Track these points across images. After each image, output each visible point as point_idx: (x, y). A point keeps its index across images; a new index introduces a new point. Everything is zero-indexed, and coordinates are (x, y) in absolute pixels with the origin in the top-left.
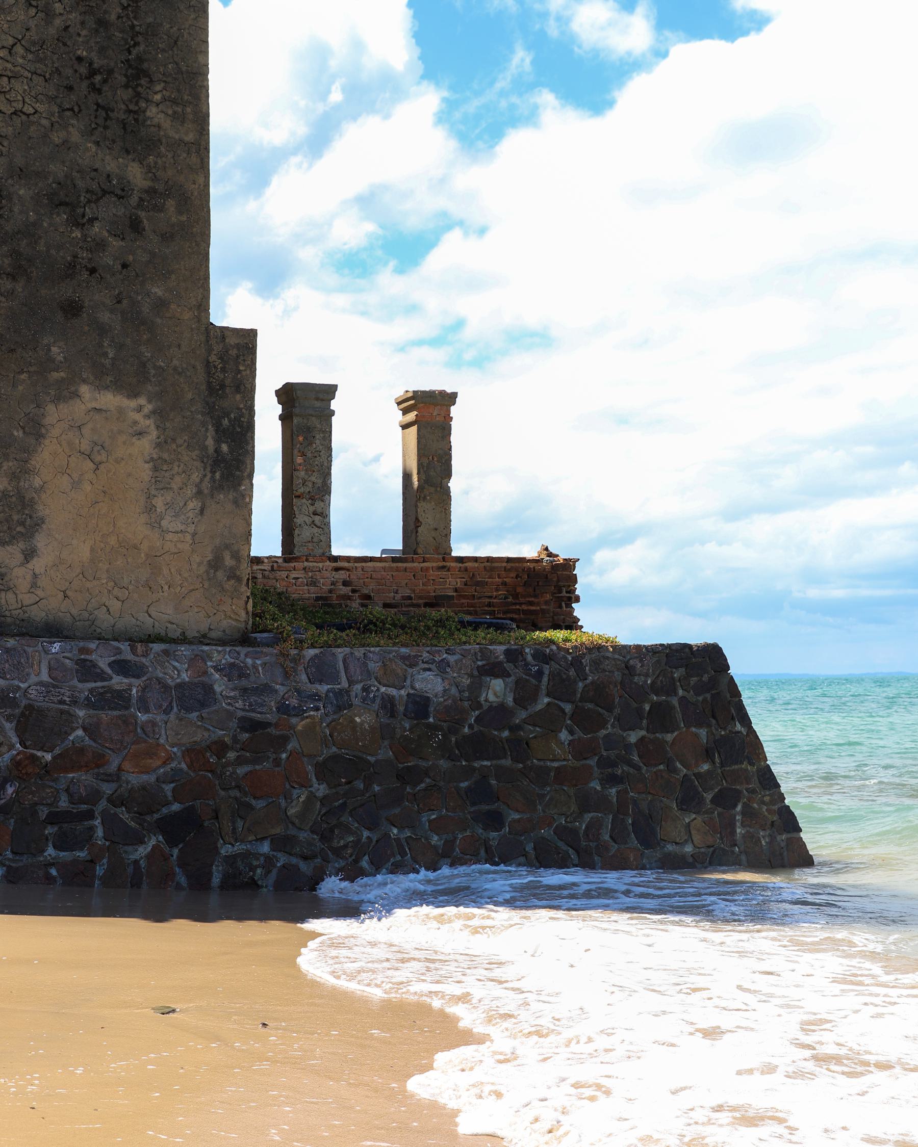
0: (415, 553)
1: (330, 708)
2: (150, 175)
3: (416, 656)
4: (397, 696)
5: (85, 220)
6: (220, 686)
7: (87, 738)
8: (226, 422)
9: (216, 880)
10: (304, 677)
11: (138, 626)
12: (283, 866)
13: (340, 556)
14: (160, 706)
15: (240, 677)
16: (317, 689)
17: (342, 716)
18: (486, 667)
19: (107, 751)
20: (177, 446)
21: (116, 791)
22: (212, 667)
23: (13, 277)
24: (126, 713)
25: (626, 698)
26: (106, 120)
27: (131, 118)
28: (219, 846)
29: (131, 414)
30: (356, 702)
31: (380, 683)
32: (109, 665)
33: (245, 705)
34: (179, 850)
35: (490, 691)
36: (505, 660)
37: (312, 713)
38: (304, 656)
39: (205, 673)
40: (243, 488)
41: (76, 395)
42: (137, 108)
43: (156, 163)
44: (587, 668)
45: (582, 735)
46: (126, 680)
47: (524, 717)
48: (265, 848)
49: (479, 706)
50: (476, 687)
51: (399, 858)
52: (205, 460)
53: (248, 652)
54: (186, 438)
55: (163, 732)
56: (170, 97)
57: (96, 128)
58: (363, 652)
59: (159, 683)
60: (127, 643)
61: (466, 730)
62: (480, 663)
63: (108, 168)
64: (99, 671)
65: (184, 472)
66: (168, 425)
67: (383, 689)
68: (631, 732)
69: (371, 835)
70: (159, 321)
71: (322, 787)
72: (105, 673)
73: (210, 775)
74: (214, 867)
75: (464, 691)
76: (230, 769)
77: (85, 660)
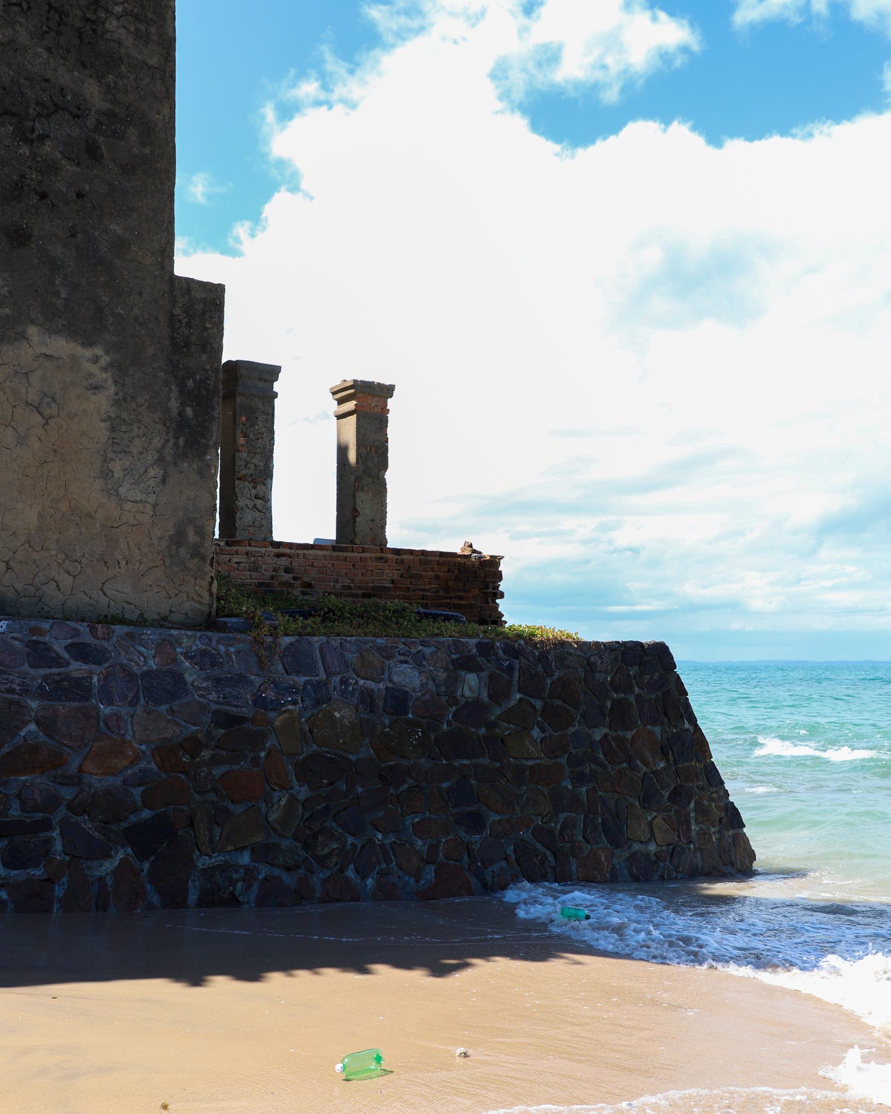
0: (352, 542)
1: (308, 702)
2: (110, 96)
3: (393, 648)
4: (376, 690)
5: (34, 136)
6: (191, 675)
7: (41, 734)
8: (190, 383)
9: (193, 897)
10: (280, 667)
11: (91, 605)
12: (265, 879)
13: (282, 542)
14: (125, 698)
15: (212, 665)
16: (294, 681)
17: (321, 710)
18: (460, 661)
19: (66, 749)
20: (137, 406)
21: (77, 796)
22: (182, 653)
24: (86, 704)
25: (590, 695)
26: (59, 24)
27: (88, 27)
28: (195, 858)
29: (86, 364)
30: (335, 695)
31: (358, 676)
32: (66, 648)
33: (219, 697)
34: (151, 864)
35: (466, 686)
36: (478, 654)
37: (290, 707)
38: (280, 645)
39: (175, 660)
40: (209, 457)
41: (23, 336)
42: (94, 17)
43: (116, 84)
44: (553, 664)
45: (552, 732)
46: (85, 667)
47: (499, 713)
48: (245, 858)
49: (456, 701)
50: (453, 681)
51: (384, 865)
52: (168, 424)
53: (221, 638)
54: (147, 397)
55: (129, 726)
56: (132, 11)
57: (47, 32)
58: (339, 642)
59: (124, 671)
60: (86, 624)
61: (445, 727)
62: (454, 656)
63: (62, 81)
64: (54, 655)
65: (145, 435)
66: (127, 380)
67: (361, 682)
68: (596, 730)
69: (355, 842)
70: (117, 262)
71: (303, 789)
72: (61, 658)
73: (183, 777)
74: (190, 882)
75: (440, 686)
76: (205, 769)
77: (40, 642)
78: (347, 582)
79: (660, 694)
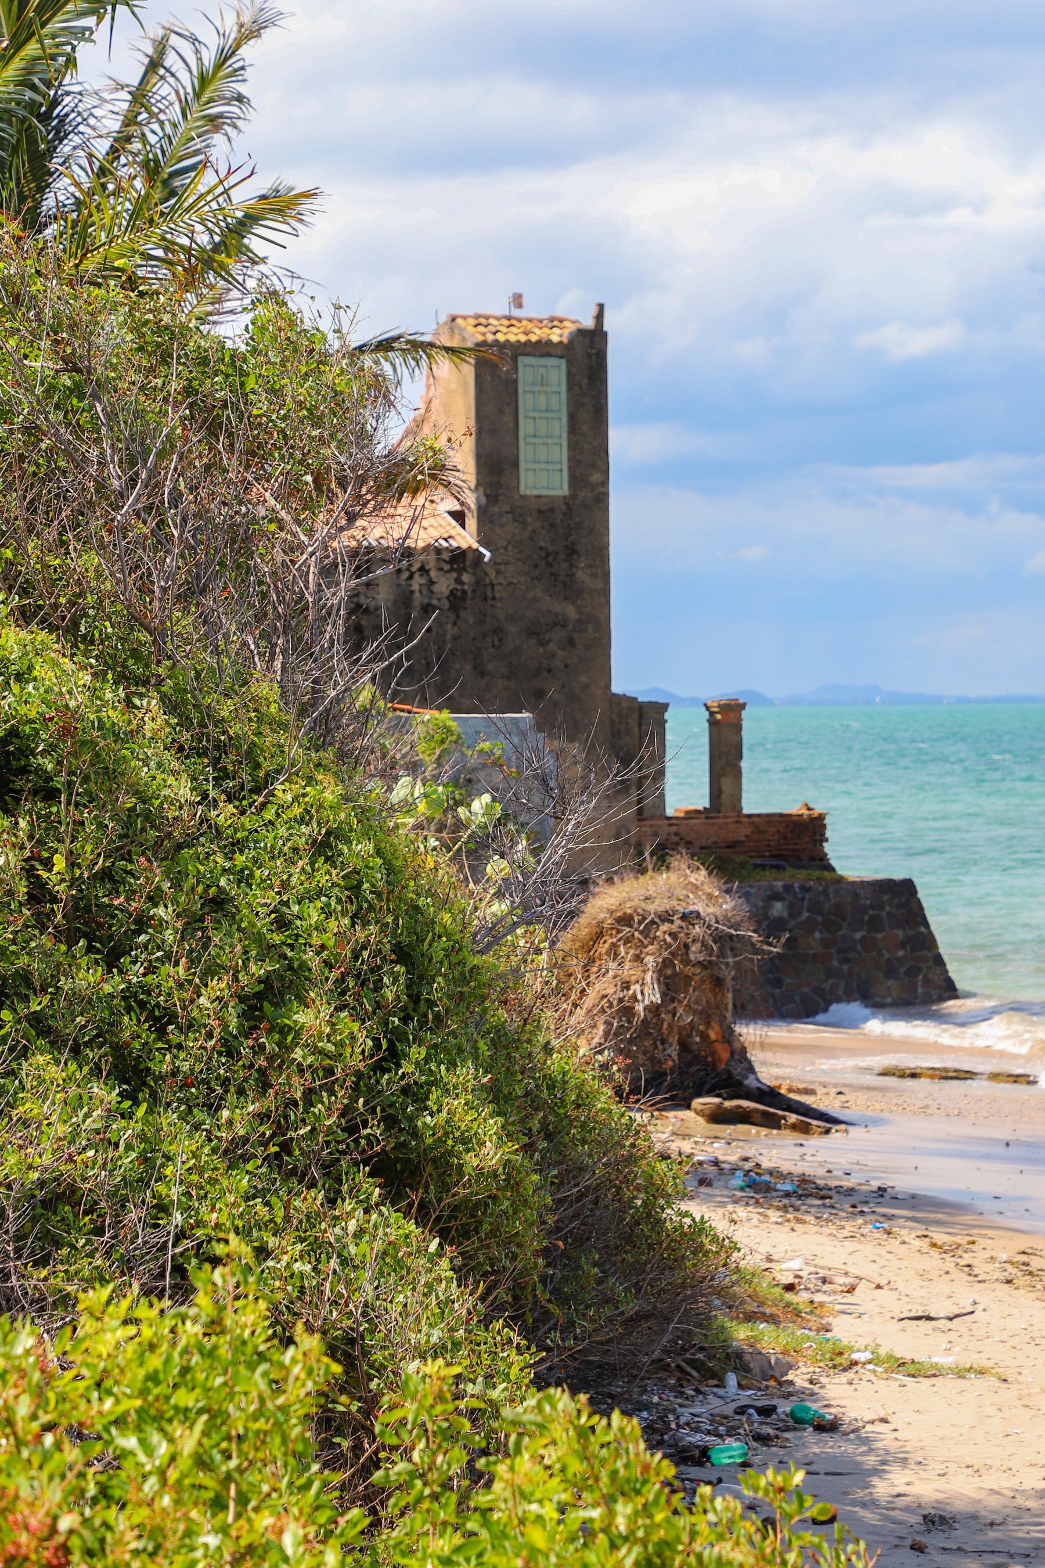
23: (508, 678)
50: (767, 907)
78: (715, 839)
79: (904, 911)
